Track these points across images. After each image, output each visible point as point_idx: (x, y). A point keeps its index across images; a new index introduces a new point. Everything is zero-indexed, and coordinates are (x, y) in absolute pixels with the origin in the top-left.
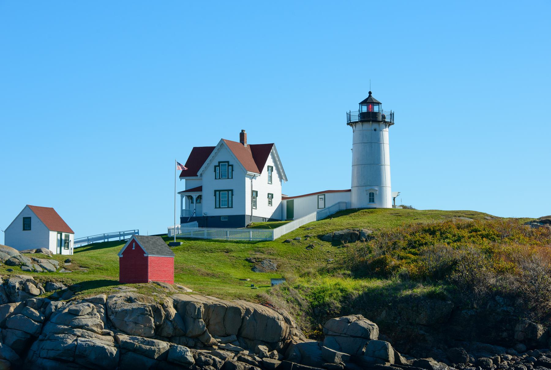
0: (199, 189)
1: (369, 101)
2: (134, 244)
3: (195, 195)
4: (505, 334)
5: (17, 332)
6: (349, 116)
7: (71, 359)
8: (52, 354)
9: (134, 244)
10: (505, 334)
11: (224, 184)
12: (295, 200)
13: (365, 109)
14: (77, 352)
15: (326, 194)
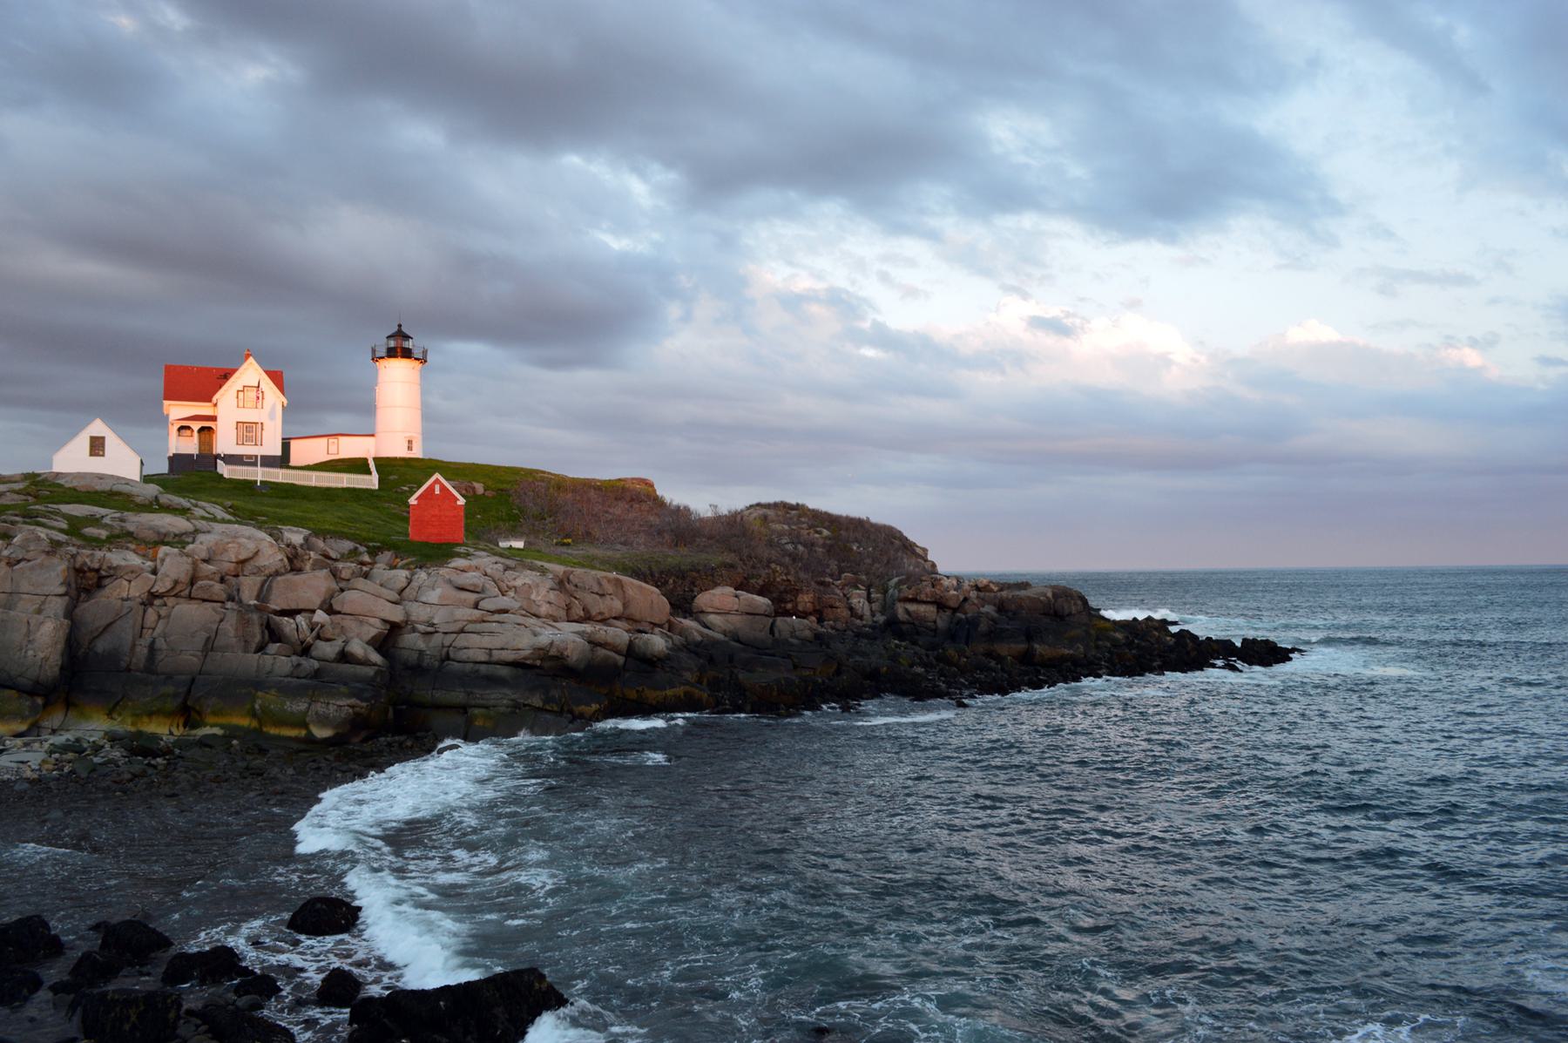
0: (213, 418)
1: (400, 335)
2: (437, 488)
3: (196, 426)
4: (789, 606)
5: (372, 620)
6: (374, 351)
7: (538, 663)
8: (509, 656)
9: (437, 488)
10: (789, 606)
11: (250, 415)
12: (293, 444)
13: (392, 344)
14: (553, 652)
15: (342, 439)
